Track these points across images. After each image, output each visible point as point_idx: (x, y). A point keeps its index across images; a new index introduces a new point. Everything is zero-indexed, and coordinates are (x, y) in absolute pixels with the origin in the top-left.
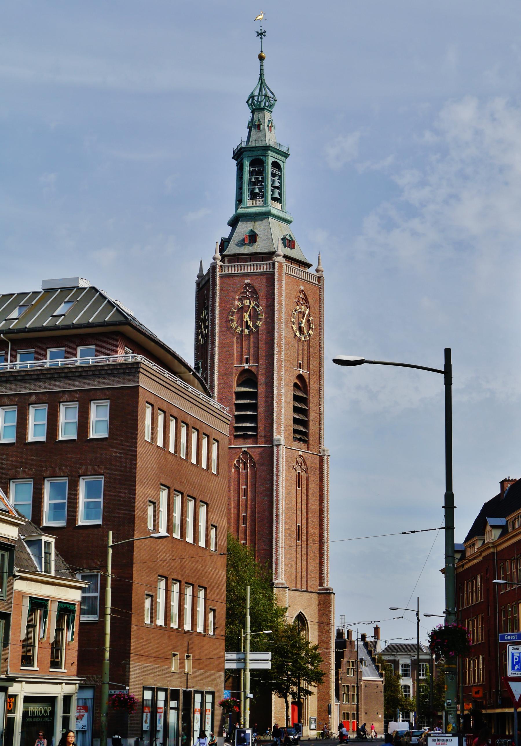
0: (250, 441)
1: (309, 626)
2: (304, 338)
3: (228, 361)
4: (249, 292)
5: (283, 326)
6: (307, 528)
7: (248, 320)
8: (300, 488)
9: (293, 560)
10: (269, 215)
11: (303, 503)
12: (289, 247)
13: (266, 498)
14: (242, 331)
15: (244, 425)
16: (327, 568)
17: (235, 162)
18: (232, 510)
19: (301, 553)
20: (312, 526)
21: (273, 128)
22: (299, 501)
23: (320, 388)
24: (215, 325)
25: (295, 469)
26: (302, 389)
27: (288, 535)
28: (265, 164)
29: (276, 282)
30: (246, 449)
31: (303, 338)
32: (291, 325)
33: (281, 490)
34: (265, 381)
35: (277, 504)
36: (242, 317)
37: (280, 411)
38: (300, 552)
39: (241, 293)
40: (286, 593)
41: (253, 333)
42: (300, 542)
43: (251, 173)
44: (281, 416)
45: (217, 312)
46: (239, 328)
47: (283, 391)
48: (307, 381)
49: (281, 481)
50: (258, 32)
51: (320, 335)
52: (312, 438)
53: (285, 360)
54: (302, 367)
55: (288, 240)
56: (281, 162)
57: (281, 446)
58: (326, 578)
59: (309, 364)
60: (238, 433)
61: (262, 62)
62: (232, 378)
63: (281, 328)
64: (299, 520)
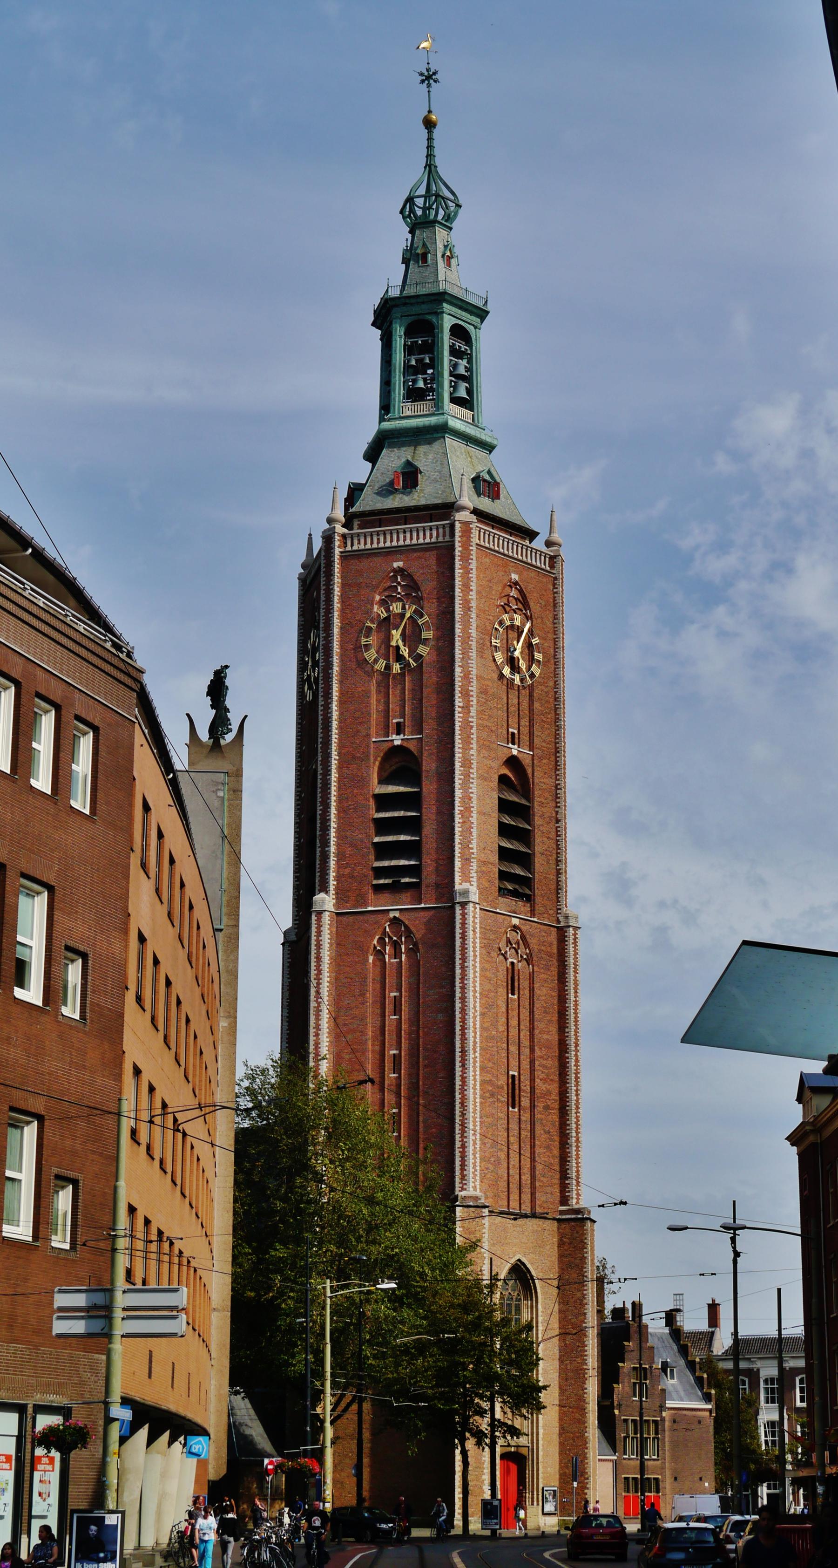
0: (406, 896)
1: (539, 1291)
2: (522, 680)
3: (358, 731)
4: (402, 586)
5: (473, 654)
6: (532, 1080)
7: (400, 643)
8: (516, 997)
9: (502, 1150)
10: (446, 432)
11: (522, 1027)
12: (489, 497)
13: (440, 1017)
14: (388, 667)
15: (394, 863)
16: (578, 1167)
17: (378, 332)
18: (370, 1043)
19: (520, 1134)
20: (542, 1076)
21: (453, 262)
22: (514, 1022)
23: (557, 787)
24: (332, 657)
25: (502, 954)
26: (519, 787)
27: (489, 1093)
28: (436, 331)
29: (458, 563)
30: (397, 914)
31: (517, 681)
32: (492, 653)
33: (471, 998)
35: (463, 1029)
36: (389, 637)
37: (467, 831)
38: (516, 1132)
39: (385, 590)
41: (411, 671)
42: (516, 1110)
43: (409, 350)
44: (470, 842)
45: (336, 631)
46: (381, 660)
47: (474, 790)
48: (529, 771)
49: (471, 980)
50: (421, 74)
51: (556, 675)
52: (539, 890)
53: (478, 725)
54: (516, 741)
55: (485, 481)
56: (472, 327)
57: (471, 905)
58: (574, 1188)
59: (531, 735)
60: (382, 881)
61: (430, 132)
62: (368, 767)
63: (469, 658)
64: (514, 1063)
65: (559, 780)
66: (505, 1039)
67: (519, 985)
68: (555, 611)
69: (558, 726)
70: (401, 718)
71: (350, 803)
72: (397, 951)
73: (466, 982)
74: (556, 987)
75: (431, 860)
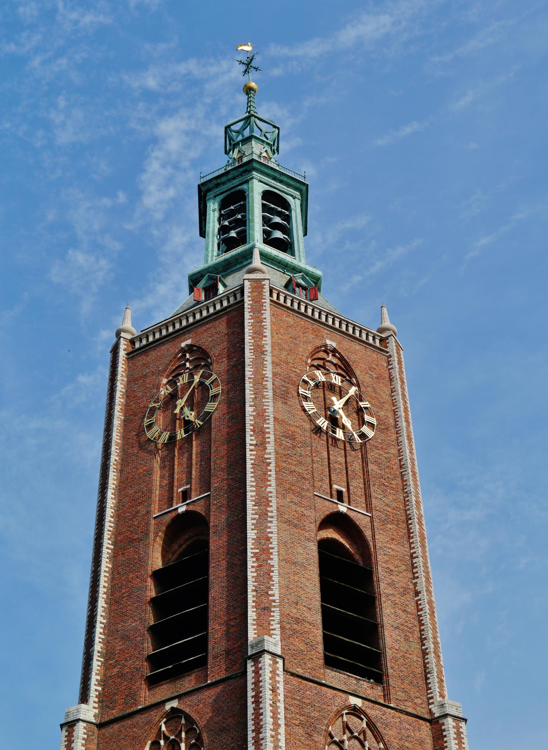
3: (137, 512)
30: (175, 704)
32: (300, 402)
34: (227, 519)
44: (269, 588)
48: (368, 533)
68: (391, 385)
69: (406, 492)
70: (187, 484)
75: (220, 624)
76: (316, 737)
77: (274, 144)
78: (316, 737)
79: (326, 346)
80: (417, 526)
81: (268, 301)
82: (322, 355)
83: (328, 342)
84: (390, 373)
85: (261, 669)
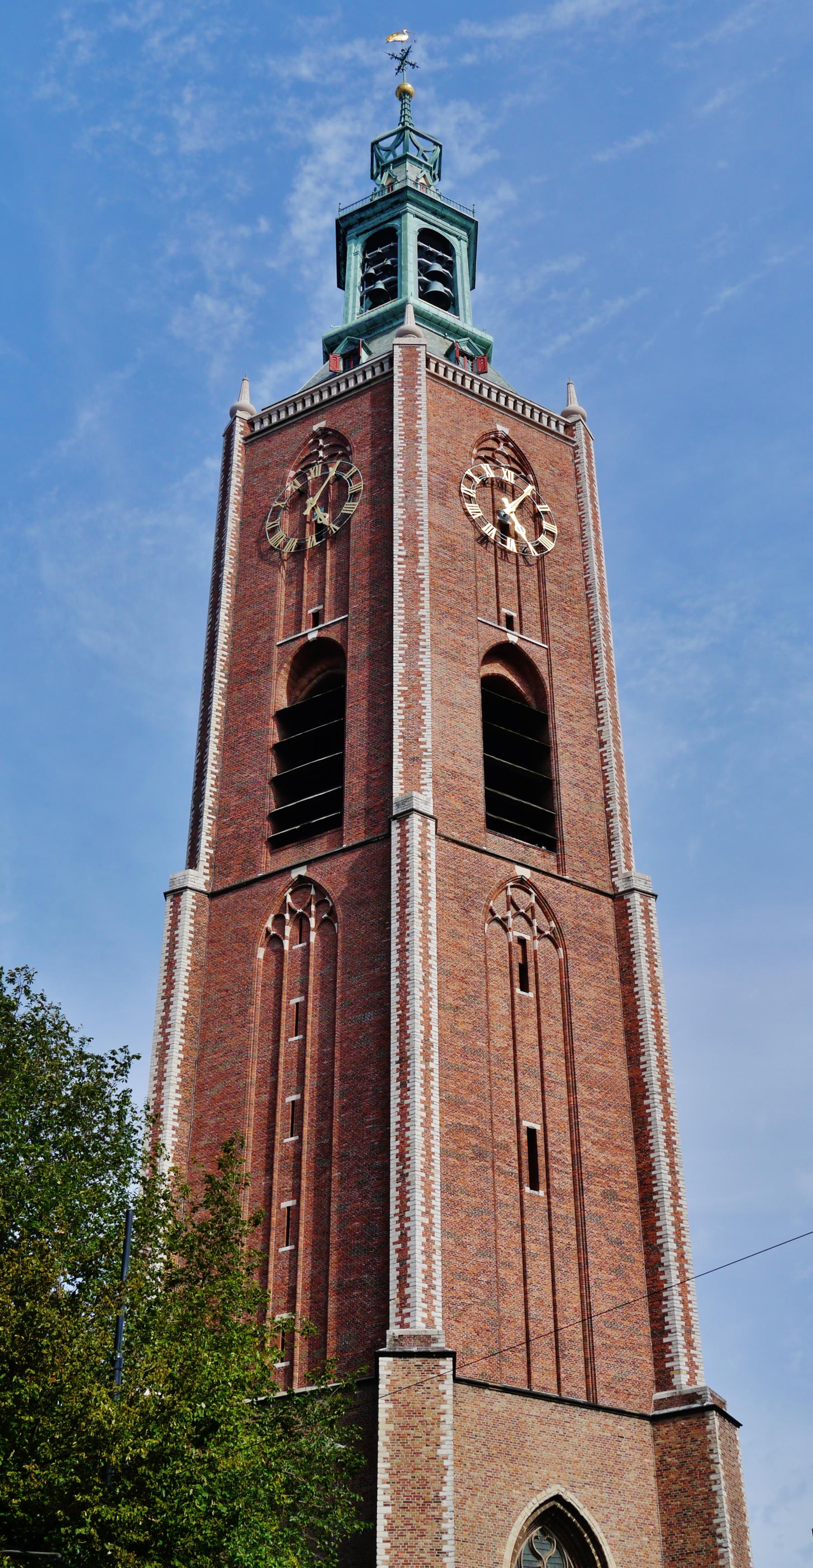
3: (257, 638)
6: (576, 1143)
16: (686, 1310)
18: (252, 1091)
22: (529, 1036)
30: (303, 871)
32: (462, 503)
34: (369, 648)
35: (403, 1019)
38: (543, 1235)
40: (441, 1378)
44: (420, 734)
48: (543, 669)
58: (682, 1351)
65: (599, 688)
66: (511, 1062)
67: (537, 975)
68: (577, 484)
69: (593, 619)
70: (319, 604)
71: (240, 735)
72: (304, 930)
73: (407, 940)
74: (618, 990)
75: (359, 777)
76: (474, 913)
77: (434, 167)
78: (474, 913)
79: (496, 432)
80: (605, 662)
81: (424, 373)
82: (491, 444)
83: (499, 428)
84: (576, 469)
85: (408, 831)
